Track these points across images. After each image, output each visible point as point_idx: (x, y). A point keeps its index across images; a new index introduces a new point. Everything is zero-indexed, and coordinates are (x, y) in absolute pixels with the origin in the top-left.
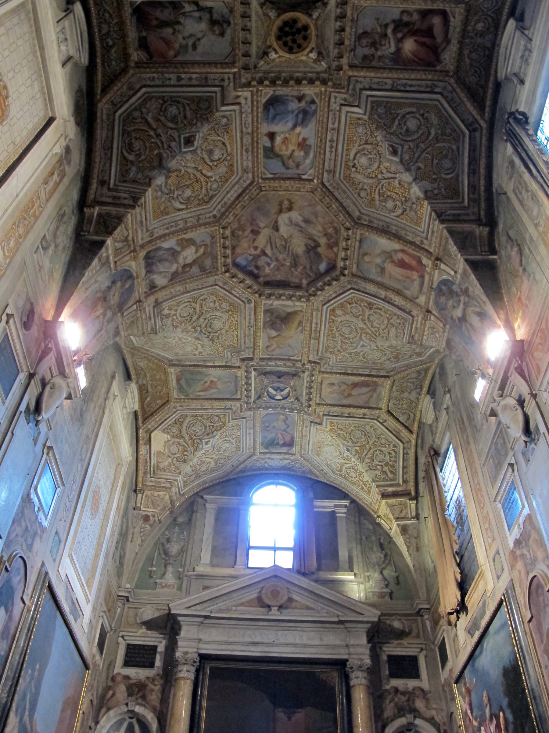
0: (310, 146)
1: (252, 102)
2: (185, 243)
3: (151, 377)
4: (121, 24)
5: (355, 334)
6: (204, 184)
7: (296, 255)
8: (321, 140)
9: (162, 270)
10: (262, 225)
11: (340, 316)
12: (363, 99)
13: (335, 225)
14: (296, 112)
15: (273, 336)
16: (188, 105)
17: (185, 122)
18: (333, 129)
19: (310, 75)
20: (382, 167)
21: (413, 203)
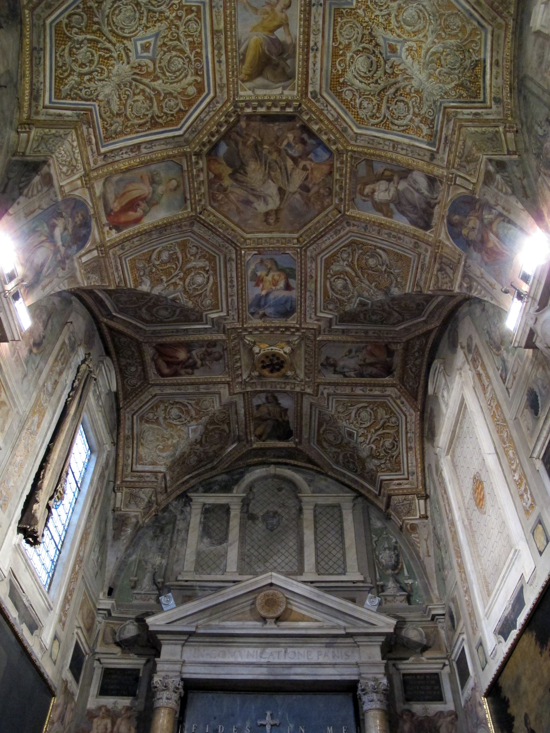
0: (251, 280)
1: (305, 315)
2: (384, 209)
4: (405, 363)
5: (162, 64)
6: (356, 263)
7: (256, 159)
8: (242, 288)
9: (416, 195)
10: (297, 196)
11: (190, 85)
13: (215, 205)
14: (267, 306)
15: (281, 30)
18: (232, 296)
21: (144, 274)
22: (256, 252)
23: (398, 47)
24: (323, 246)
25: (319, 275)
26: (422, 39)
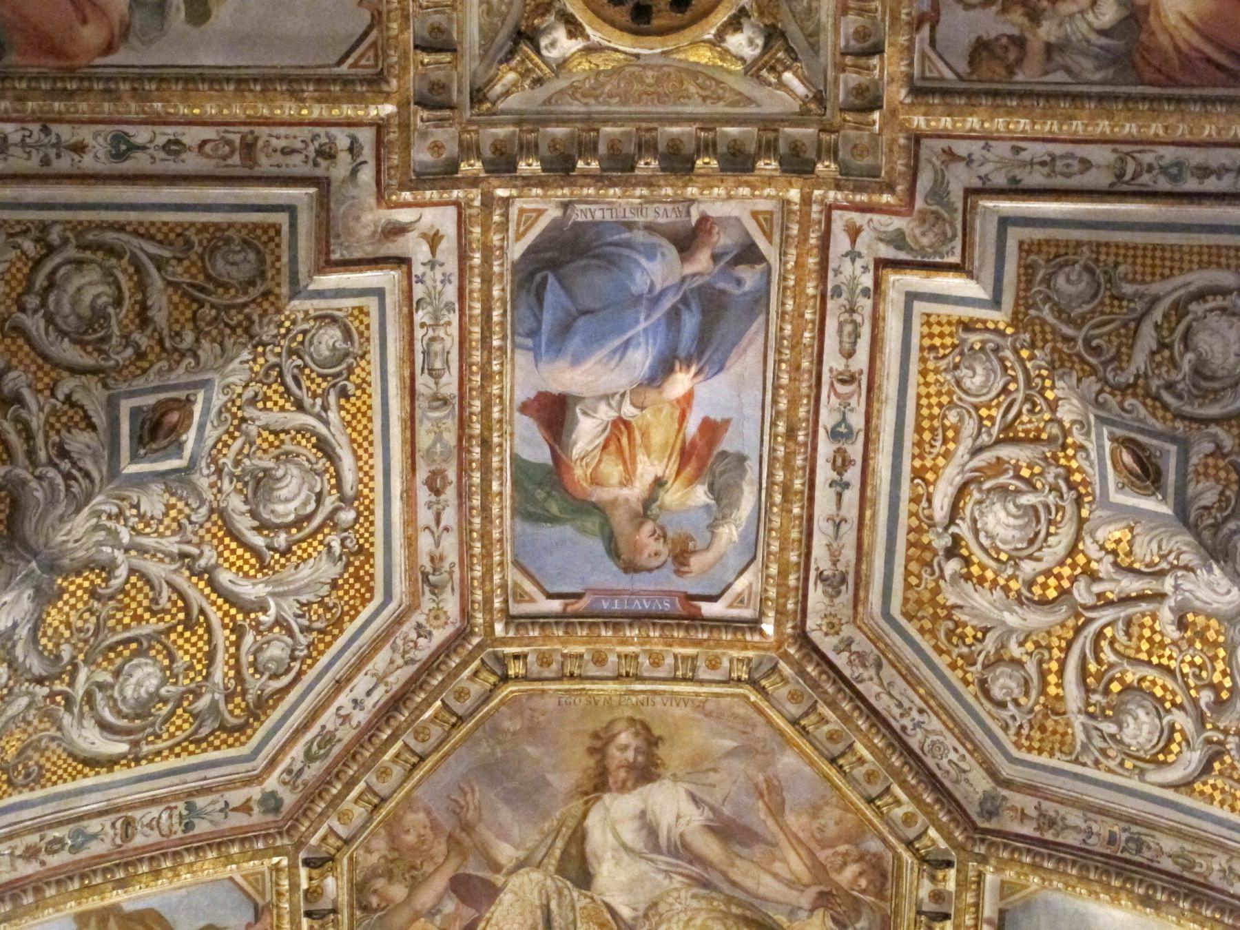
0: (742, 459)
1: (463, 257)
8: (791, 433)
10: (506, 853)
12: (985, 232)
13: (874, 845)
14: (668, 303)
16: (160, 264)
17: (144, 342)
18: (849, 379)
19: (732, 130)
20: (1088, 545)
22: (708, 609)
24: (380, 660)
25: (397, 506)
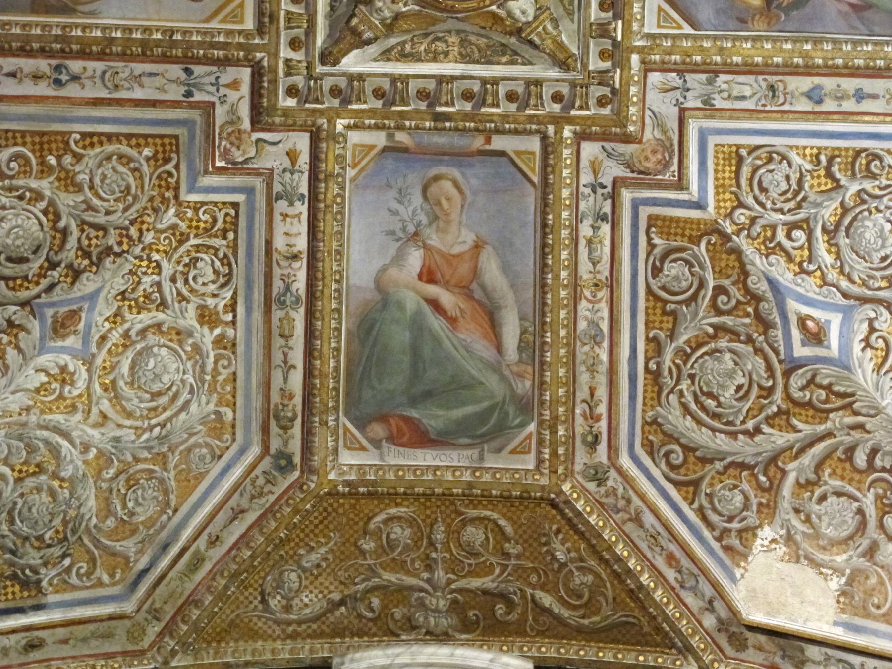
3: (399, 566)
23: (71, 341)
26: (95, 410)
